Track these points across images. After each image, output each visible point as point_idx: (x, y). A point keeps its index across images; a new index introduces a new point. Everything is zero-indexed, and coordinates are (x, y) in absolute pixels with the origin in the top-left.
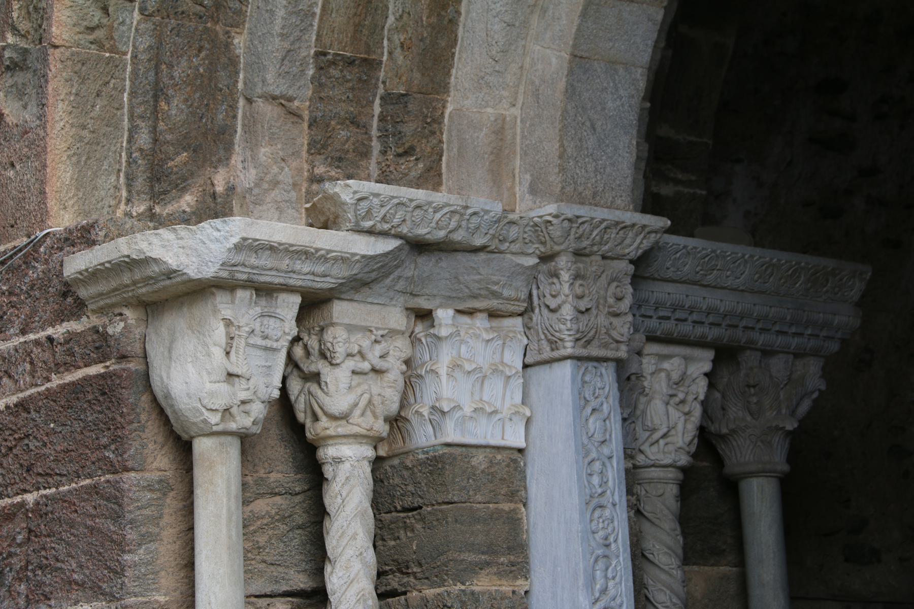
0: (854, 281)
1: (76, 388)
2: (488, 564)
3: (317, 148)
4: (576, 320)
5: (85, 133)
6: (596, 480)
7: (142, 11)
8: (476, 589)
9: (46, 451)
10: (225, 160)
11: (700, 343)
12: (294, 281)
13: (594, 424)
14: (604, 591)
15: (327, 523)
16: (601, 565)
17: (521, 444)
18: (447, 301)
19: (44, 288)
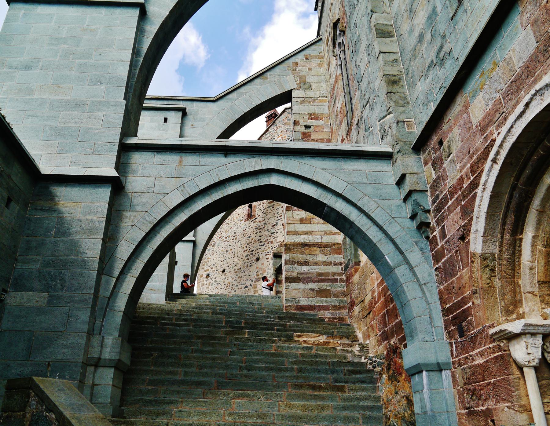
1: (496, 357)
3: (542, 302)
10: (522, 306)
12: (540, 332)
19: (487, 337)
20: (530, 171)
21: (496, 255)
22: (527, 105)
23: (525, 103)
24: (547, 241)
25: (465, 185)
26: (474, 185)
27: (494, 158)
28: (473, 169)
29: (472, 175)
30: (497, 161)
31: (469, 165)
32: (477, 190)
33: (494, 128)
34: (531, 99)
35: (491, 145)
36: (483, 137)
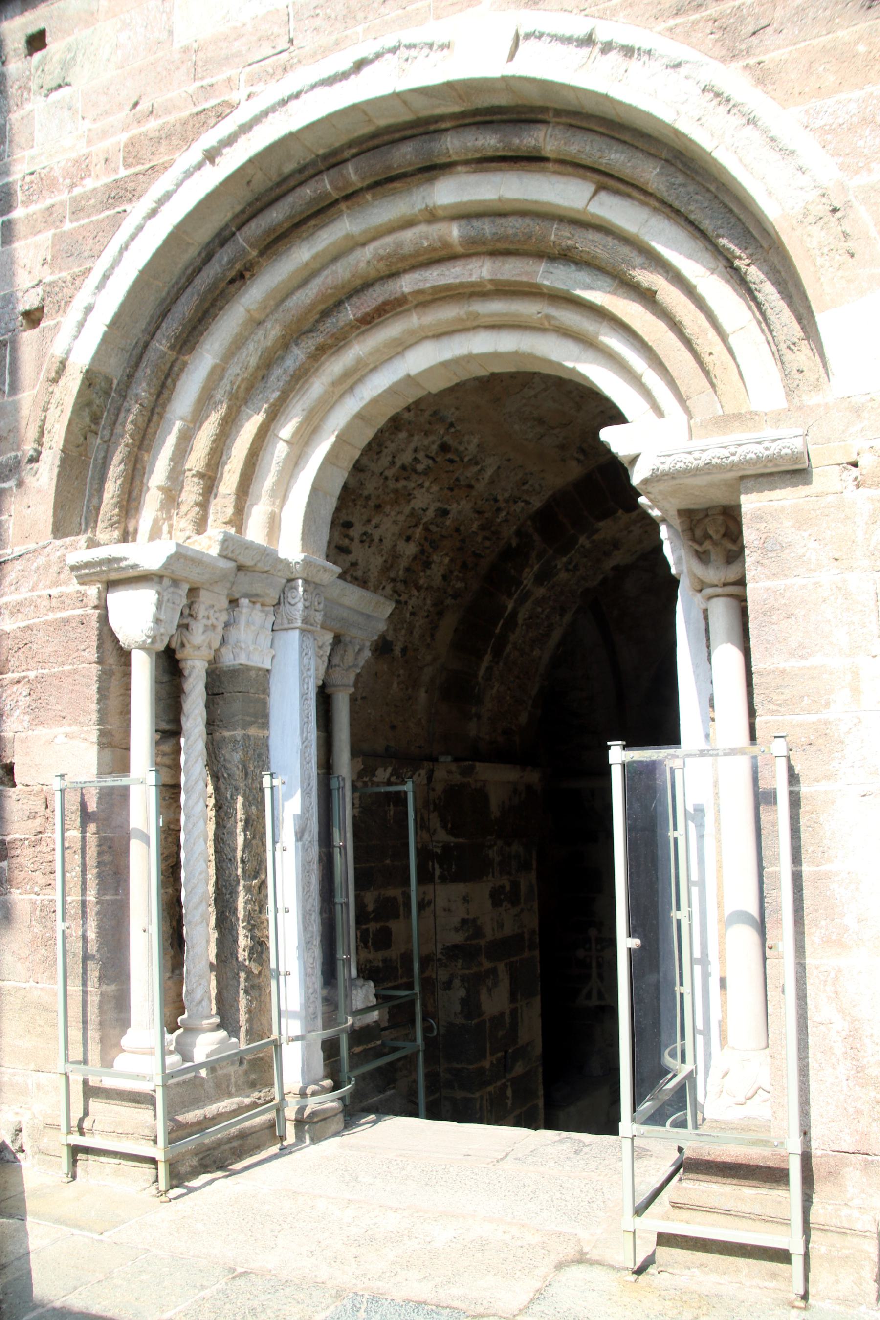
0: (388, 608)
1: (66, 621)
2: (254, 722)
4: (303, 611)
5: (69, 495)
6: (305, 687)
7: (102, 438)
8: (250, 734)
9: (43, 650)
11: (330, 630)
13: (306, 661)
14: (306, 739)
15: (183, 697)
16: (306, 725)
17: (269, 667)
18: (246, 596)
20: (281, 217)
21: (115, 382)
22: (360, 65)
23: (358, 57)
24: (239, 387)
25: (90, 184)
26: (120, 194)
27: (213, 148)
28: (132, 152)
29: (127, 166)
30: (217, 160)
31: (124, 137)
32: (128, 207)
33: (243, 77)
34: (378, 56)
35: (221, 113)
36: (198, 84)
